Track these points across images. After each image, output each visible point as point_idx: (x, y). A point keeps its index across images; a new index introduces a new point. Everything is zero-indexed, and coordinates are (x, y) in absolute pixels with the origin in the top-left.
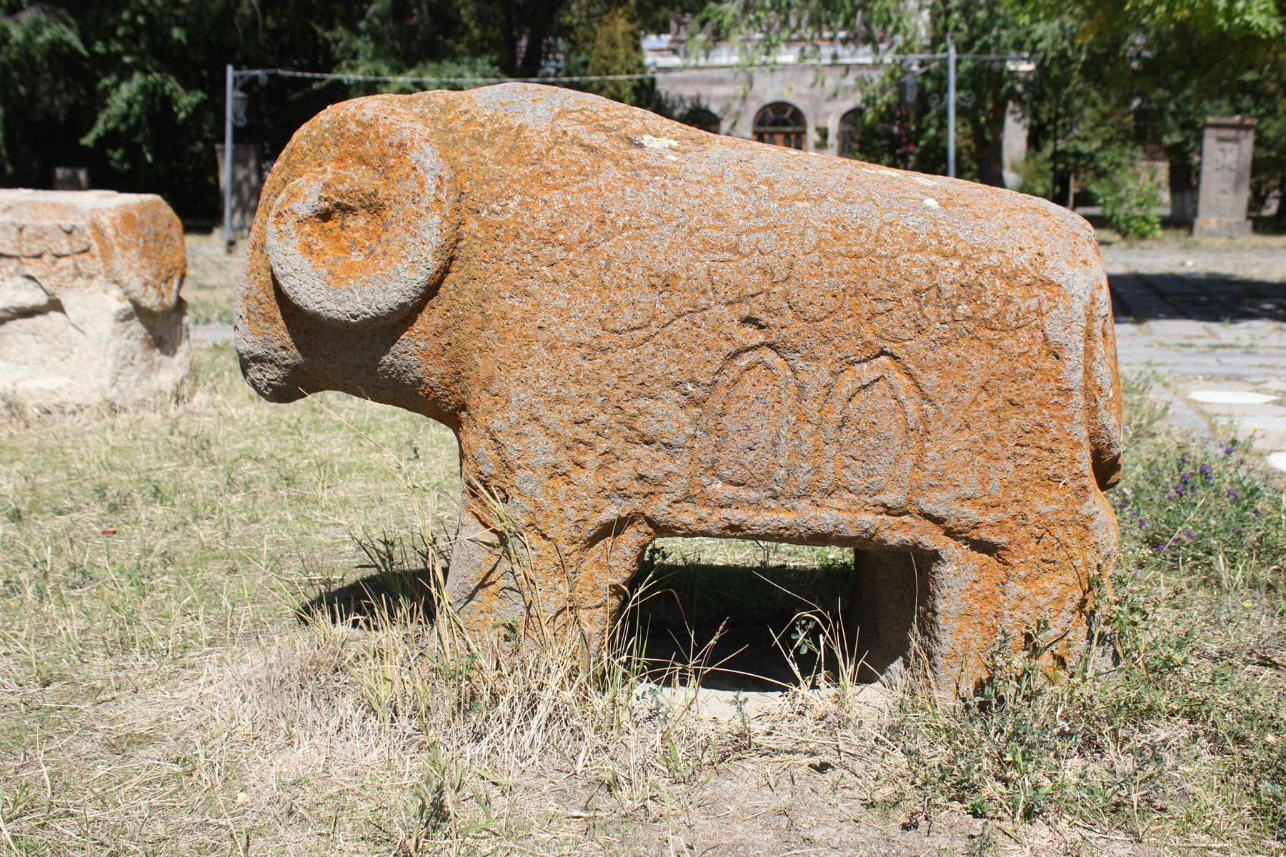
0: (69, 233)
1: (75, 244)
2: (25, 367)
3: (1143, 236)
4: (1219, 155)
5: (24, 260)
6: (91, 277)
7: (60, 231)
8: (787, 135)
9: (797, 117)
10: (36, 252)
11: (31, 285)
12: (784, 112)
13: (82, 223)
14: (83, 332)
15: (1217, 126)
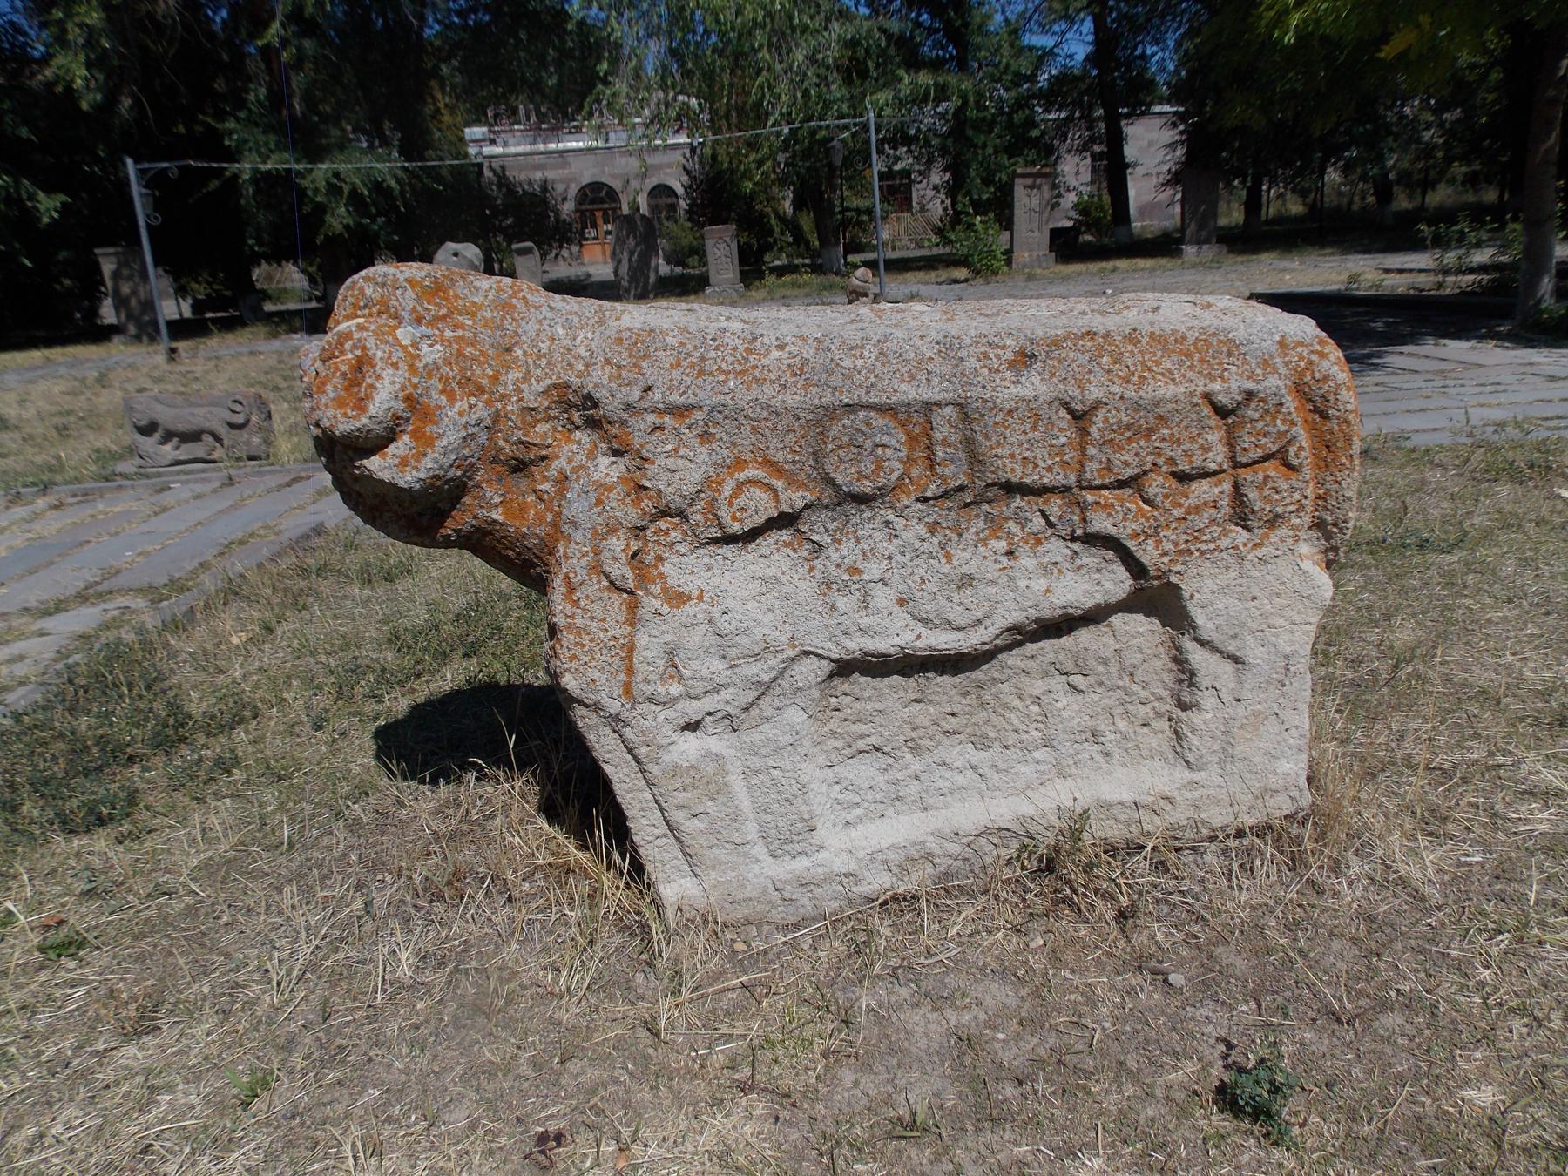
0: (1222, 412)
1: (1246, 441)
2: (1042, 754)
3: (995, 273)
4: (1026, 200)
5: (1089, 497)
6: (1274, 521)
7: (1207, 411)
8: (605, 211)
9: (612, 195)
10: (1130, 472)
11: (1090, 557)
12: (600, 190)
13: (1275, 383)
14: (1235, 659)
15: (1023, 176)
